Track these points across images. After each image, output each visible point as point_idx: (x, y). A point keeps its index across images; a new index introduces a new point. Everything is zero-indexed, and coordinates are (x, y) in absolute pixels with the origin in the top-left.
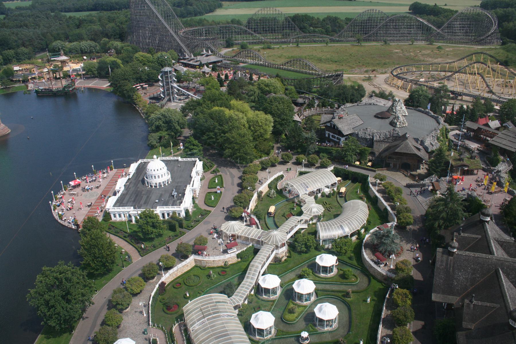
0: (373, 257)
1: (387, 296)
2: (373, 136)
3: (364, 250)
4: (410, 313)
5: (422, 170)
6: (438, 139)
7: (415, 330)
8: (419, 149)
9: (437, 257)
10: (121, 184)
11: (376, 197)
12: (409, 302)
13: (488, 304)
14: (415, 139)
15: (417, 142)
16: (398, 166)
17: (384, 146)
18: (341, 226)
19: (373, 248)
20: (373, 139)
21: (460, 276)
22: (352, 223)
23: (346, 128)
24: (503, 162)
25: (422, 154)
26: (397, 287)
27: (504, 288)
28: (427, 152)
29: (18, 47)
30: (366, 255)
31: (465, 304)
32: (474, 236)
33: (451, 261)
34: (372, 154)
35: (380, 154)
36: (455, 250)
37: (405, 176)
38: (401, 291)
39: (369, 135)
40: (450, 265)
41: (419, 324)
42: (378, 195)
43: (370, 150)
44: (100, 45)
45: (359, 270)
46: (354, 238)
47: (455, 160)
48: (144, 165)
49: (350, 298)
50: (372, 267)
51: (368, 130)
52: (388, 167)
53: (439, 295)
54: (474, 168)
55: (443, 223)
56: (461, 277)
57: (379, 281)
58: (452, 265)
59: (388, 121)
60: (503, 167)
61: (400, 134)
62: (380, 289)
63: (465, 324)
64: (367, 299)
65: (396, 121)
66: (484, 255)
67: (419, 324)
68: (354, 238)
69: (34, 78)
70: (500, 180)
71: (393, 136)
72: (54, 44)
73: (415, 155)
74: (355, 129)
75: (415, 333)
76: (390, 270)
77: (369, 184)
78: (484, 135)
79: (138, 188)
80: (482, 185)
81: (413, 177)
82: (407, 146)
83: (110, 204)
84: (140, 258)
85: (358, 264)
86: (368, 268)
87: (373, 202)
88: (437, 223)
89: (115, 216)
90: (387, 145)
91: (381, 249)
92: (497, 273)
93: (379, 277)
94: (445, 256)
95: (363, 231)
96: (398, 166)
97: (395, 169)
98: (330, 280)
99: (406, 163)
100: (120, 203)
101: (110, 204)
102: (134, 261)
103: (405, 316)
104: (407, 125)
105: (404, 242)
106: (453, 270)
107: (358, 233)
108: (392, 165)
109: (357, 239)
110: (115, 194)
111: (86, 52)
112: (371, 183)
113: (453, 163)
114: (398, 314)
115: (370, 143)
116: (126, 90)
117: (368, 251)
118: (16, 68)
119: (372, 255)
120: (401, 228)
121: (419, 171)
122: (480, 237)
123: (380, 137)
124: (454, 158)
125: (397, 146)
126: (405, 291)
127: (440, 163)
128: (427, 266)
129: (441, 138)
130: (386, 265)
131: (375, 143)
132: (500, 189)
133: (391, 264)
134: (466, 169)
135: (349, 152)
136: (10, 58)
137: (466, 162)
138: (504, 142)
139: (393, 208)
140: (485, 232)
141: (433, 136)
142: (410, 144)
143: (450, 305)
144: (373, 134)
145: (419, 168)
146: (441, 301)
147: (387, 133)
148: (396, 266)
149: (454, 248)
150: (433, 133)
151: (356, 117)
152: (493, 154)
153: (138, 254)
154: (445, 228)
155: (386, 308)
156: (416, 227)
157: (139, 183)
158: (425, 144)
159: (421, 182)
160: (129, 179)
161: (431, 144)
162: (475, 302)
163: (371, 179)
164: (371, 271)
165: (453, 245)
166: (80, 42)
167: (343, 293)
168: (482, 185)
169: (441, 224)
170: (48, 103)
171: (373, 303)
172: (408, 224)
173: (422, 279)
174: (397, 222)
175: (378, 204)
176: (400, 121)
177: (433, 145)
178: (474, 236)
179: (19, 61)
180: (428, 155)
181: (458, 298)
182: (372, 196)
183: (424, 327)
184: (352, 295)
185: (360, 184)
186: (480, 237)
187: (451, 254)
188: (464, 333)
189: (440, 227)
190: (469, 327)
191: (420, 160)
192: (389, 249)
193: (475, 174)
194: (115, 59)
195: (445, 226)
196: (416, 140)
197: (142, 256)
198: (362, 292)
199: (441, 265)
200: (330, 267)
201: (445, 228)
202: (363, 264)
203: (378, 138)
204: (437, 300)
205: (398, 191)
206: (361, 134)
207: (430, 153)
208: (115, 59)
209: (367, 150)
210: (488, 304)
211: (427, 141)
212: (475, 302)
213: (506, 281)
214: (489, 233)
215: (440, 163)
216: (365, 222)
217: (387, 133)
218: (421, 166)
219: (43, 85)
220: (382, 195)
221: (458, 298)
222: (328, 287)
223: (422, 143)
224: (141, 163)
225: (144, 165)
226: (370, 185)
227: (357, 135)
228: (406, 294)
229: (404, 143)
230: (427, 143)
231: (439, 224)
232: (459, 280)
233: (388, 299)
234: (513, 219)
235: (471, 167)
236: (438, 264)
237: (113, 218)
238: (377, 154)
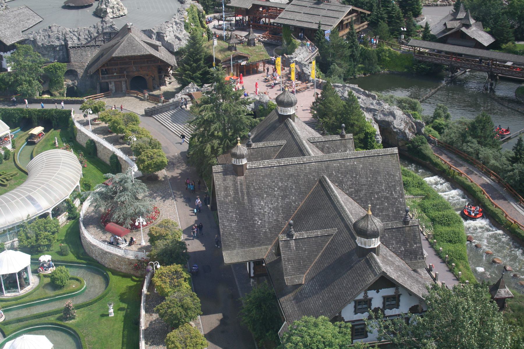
0: (104, 237)
1: (145, 290)
2: (65, 40)
3: (83, 228)
4: (192, 301)
5: (171, 85)
6: (187, 27)
7: (206, 332)
8: (156, 47)
9: (216, 183)
11: (92, 142)
12: (186, 285)
13: (319, 233)
14: (144, 31)
15: (151, 37)
16: (124, 86)
17: (90, 55)
18: (30, 198)
19: (101, 221)
20: (66, 44)
21: (263, 208)
22: (51, 188)
23: (8, 33)
24: (303, 45)
25: (163, 55)
26: (159, 266)
27: (338, 201)
28: (172, 52)
30: (92, 237)
31: (281, 244)
32: (274, 143)
33: (241, 184)
34: (71, 73)
35: (86, 71)
36: (244, 161)
37: (141, 100)
38: (165, 269)
39: (58, 39)
40: (242, 192)
41: (214, 320)
42: (95, 137)
43: (65, 67)
45: (81, 267)
46: (62, 219)
47: (222, 50)
49: (74, 318)
50: (106, 253)
51: (54, 29)
52: (106, 91)
53: (235, 252)
54: (257, 59)
55: (219, 144)
56: (266, 209)
57: (125, 276)
58: (245, 191)
59: (89, 11)
60: (304, 54)
61: (118, 27)
62: (130, 288)
63: (289, 280)
64: (108, 309)
65: (104, 6)
66: (295, 160)
67: (214, 320)
68: (62, 219)
70: (303, 70)
71: (105, 34)
73: (151, 57)
74: (27, 32)
75: (210, 336)
76: (141, 249)
77: (73, 124)
78: (266, 17)
80: (275, 84)
81: (155, 99)
82: (132, 43)
85: (78, 258)
86: (99, 259)
87: (89, 152)
88: (208, 146)
90: (96, 52)
91: (115, 216)
92: (322, 183)
93: (124, 268)
94: (230, 178)
95: (77, 203)
96: (124, 86)
97: (119, 93)
98: (27, 299)
99: (138, 74)
103: (182, 306)
104: (126, 12)
105: (158, 199)
106: (250, 201)
107: (67, 207)
108: (112, 86)
109: (69, 219)
112: (78, 122)
113: (220, 56)
114: (169, 308)
115: (64, 52)
117: (93, 229)
119: (101, 234)
120: (148, 177)
121: (163, 88)
122: (284, 142)
123: (79, 39)
124: (220, 48)
125: (113, 48)
126: (175, 267)
127: (197, 61)
128: (206, 227)
129: (193, 26)
130: (131, 242)
131: (72, 52)
132: (304, 85)
133: (140, 240)
134: (244, 63)
135: (23, 74)
137: (241, 50)
138: (298, 17)
139: (127, 152)
140: (290, 132)
141: (176, 23)
142: (137, 38)
143: (258, 263)
144: (65, 35)
145: (164, 84)
146: (240, 260)
147: (92, 30)
148: (150, 234)
149: (242, 157)
150: (176, 17)
151: (26, 11)
152: (285, 42)
154: (224, 153)
155: (146, 312)
156: (176, 173)
158: (166, 39)
159: (171, 101)
161: (177, 37)
162: (296, 235)
163: (76, 116)
164: (106, 262)
165: (238, 152)
167: (58, 315)
168: (275, 84)
169: (216, 145)
171: (122, 313)
172: (160, 166)
173: (203, 248)
174: (139, 169)
175: (99, 155)
176: (111, 5)
177: (179, 39)
178: (274, 143)
180: (174, 57)
181: (270, 247)
182: (83, 142)
183: (222, 322)
184: (77, 313)
185: (58, 132)
186: (284, 142)
187: (237, 171)
188: (291, 296)
189: (214, 151)
190: (297, 282)
191: (162, 68)
192: (131, 211)
193: (260, 72)
195: (223, 149)
196: (148, 33)
198: (96, 301)
199: (226, 196)
200: (20, 273)
201: (224, 153)
202: (88, 255)
203: (76, 41)
204: (235, 260)
205: (131, 119)
206: (41, 40)
207: (177, 54)
209: (60, 68)
210: (319, 233)
211: (167, 33)
212: (296, 235)
213: (339, 193)
214: (299, 132)
215: (197, 61)
216: (78, 184)
217: (92, 30)
218: (167, 80)
220: (102, 136)
221: (270, 247)
222: (24, 313)
223: (160, 36)
226: (78, 125)
227: (34, 42)
228: (176, 272)
229: (126, 38)
230: (169, 37)
231: (212, 147)
232: (264, 215)
233: (147, 296)
234: (334, 118)
235: (253, 59)
236: (220, 195)
238: (81, 72)
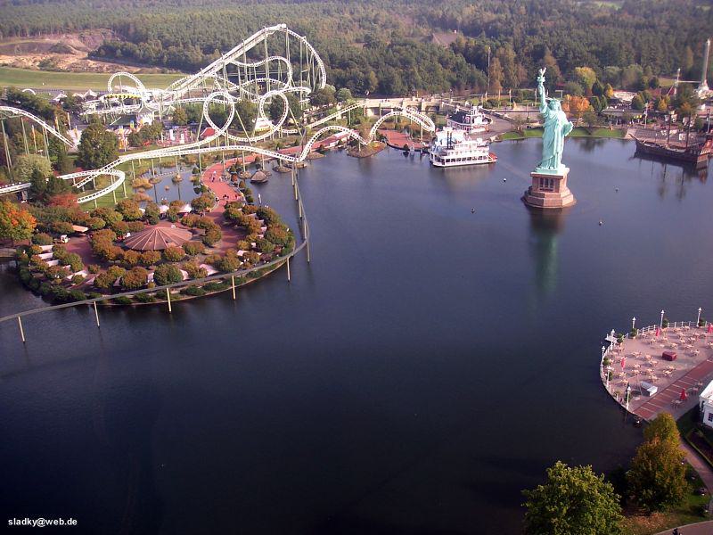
170: (651, 167)
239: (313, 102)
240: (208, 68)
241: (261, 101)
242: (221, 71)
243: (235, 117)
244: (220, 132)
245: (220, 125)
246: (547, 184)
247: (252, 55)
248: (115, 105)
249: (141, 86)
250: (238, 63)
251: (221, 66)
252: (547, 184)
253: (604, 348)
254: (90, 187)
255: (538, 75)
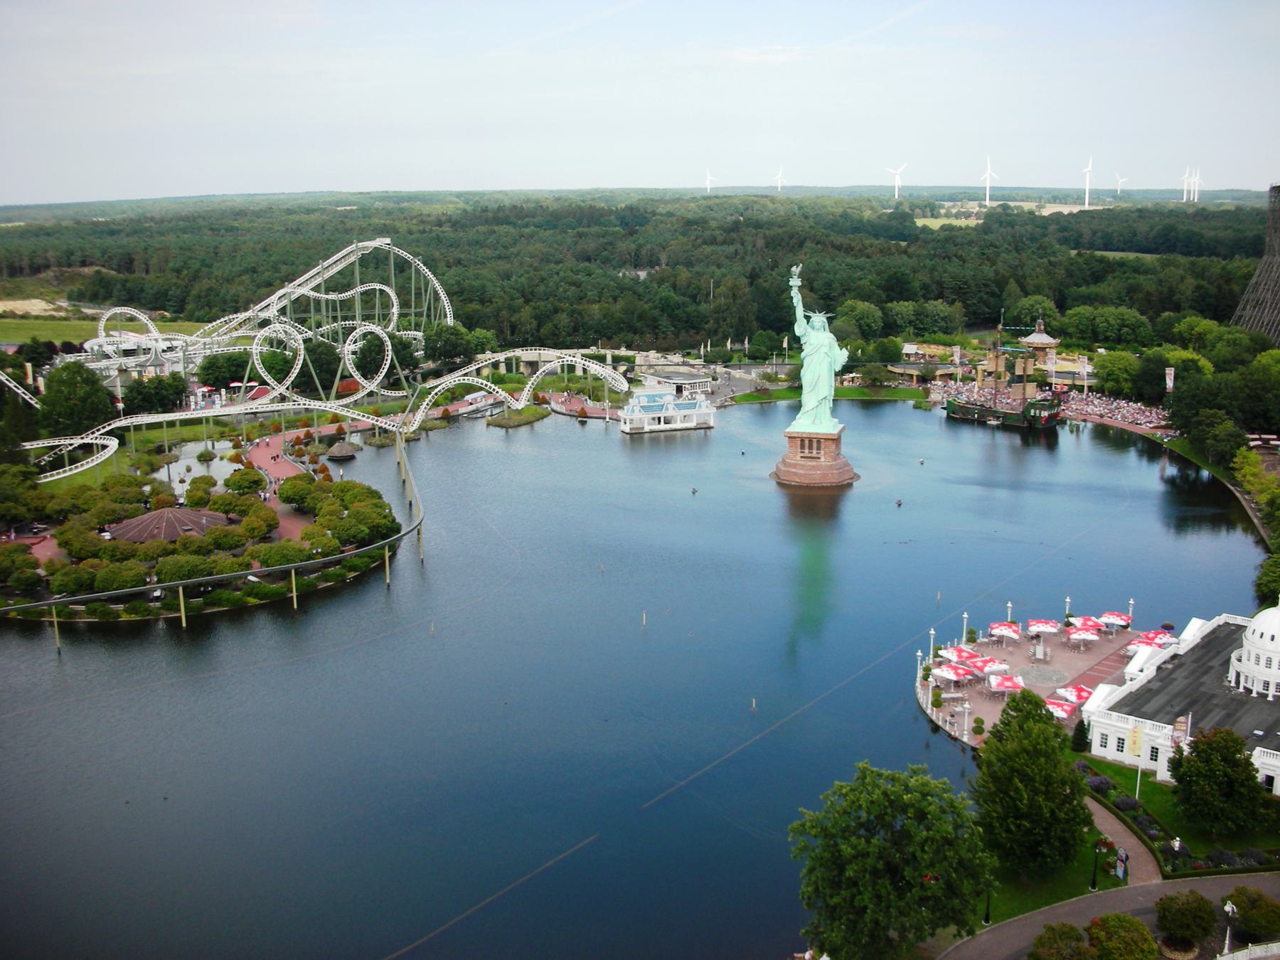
10: (1144, 661)
29: (927, 299)
44: (1154, 325)
48: (1234, 632)
69: (951, 376)
72: (1026, 302)
79: (1202, 684)
83: (1101, 698)
84: (1158, 880)
89: (1104, 745)
100: (1134, 705)
101: (1098, 704)
102: (1133, 883)
110: (1121, 682)
111: (1106, 339)
116: (1215, 437)
118: (909, 348)
136: (899, 322)
153: (1151, 867)
157: (1206, 673)
160: (1175, 657)
166: (1096, 308)
170: (972, 441)
179: (921, 332)
194: (1195, 356)
197: (1165, 877)
208: (1195, 356)
219: (974, 393)
224: (1227, 624)
225: (1234, 632)
237: (1096, 750)
239: (431, 354)
240: (263, 304)
241: (348, 351)
242: (283, 311)
243: (305, 364)
244: (281, 389)
245: (280, 381)
246: (810, 447)
247: (340, 283)
248: (108, 357)
249: (155, 333)
250: (313, 294)
251: (285, 302)
252: (810, 447)
253: (919, 653)
254: (57, 464)
255: (789, 275)
